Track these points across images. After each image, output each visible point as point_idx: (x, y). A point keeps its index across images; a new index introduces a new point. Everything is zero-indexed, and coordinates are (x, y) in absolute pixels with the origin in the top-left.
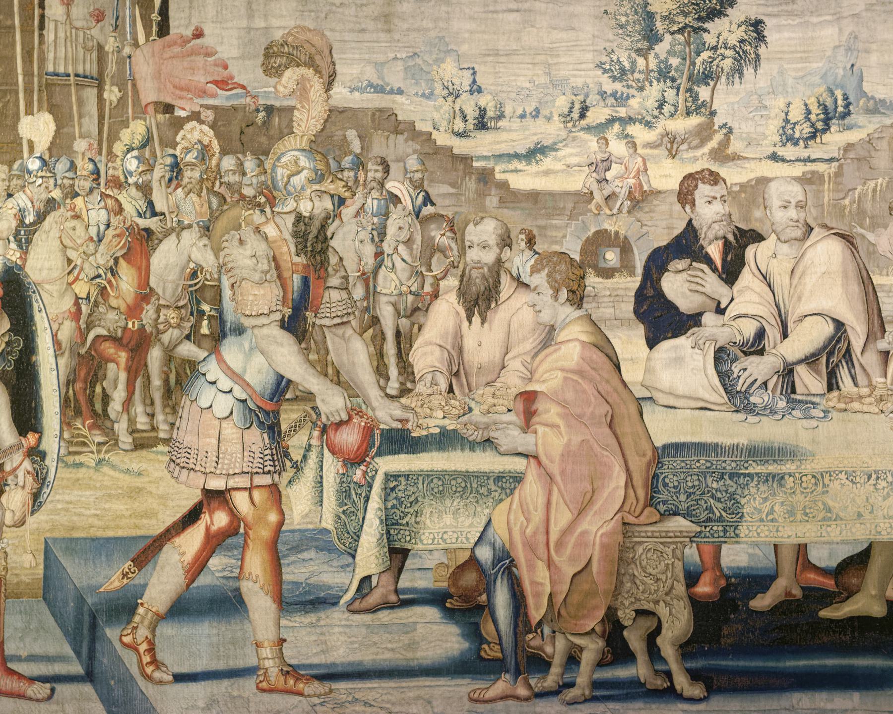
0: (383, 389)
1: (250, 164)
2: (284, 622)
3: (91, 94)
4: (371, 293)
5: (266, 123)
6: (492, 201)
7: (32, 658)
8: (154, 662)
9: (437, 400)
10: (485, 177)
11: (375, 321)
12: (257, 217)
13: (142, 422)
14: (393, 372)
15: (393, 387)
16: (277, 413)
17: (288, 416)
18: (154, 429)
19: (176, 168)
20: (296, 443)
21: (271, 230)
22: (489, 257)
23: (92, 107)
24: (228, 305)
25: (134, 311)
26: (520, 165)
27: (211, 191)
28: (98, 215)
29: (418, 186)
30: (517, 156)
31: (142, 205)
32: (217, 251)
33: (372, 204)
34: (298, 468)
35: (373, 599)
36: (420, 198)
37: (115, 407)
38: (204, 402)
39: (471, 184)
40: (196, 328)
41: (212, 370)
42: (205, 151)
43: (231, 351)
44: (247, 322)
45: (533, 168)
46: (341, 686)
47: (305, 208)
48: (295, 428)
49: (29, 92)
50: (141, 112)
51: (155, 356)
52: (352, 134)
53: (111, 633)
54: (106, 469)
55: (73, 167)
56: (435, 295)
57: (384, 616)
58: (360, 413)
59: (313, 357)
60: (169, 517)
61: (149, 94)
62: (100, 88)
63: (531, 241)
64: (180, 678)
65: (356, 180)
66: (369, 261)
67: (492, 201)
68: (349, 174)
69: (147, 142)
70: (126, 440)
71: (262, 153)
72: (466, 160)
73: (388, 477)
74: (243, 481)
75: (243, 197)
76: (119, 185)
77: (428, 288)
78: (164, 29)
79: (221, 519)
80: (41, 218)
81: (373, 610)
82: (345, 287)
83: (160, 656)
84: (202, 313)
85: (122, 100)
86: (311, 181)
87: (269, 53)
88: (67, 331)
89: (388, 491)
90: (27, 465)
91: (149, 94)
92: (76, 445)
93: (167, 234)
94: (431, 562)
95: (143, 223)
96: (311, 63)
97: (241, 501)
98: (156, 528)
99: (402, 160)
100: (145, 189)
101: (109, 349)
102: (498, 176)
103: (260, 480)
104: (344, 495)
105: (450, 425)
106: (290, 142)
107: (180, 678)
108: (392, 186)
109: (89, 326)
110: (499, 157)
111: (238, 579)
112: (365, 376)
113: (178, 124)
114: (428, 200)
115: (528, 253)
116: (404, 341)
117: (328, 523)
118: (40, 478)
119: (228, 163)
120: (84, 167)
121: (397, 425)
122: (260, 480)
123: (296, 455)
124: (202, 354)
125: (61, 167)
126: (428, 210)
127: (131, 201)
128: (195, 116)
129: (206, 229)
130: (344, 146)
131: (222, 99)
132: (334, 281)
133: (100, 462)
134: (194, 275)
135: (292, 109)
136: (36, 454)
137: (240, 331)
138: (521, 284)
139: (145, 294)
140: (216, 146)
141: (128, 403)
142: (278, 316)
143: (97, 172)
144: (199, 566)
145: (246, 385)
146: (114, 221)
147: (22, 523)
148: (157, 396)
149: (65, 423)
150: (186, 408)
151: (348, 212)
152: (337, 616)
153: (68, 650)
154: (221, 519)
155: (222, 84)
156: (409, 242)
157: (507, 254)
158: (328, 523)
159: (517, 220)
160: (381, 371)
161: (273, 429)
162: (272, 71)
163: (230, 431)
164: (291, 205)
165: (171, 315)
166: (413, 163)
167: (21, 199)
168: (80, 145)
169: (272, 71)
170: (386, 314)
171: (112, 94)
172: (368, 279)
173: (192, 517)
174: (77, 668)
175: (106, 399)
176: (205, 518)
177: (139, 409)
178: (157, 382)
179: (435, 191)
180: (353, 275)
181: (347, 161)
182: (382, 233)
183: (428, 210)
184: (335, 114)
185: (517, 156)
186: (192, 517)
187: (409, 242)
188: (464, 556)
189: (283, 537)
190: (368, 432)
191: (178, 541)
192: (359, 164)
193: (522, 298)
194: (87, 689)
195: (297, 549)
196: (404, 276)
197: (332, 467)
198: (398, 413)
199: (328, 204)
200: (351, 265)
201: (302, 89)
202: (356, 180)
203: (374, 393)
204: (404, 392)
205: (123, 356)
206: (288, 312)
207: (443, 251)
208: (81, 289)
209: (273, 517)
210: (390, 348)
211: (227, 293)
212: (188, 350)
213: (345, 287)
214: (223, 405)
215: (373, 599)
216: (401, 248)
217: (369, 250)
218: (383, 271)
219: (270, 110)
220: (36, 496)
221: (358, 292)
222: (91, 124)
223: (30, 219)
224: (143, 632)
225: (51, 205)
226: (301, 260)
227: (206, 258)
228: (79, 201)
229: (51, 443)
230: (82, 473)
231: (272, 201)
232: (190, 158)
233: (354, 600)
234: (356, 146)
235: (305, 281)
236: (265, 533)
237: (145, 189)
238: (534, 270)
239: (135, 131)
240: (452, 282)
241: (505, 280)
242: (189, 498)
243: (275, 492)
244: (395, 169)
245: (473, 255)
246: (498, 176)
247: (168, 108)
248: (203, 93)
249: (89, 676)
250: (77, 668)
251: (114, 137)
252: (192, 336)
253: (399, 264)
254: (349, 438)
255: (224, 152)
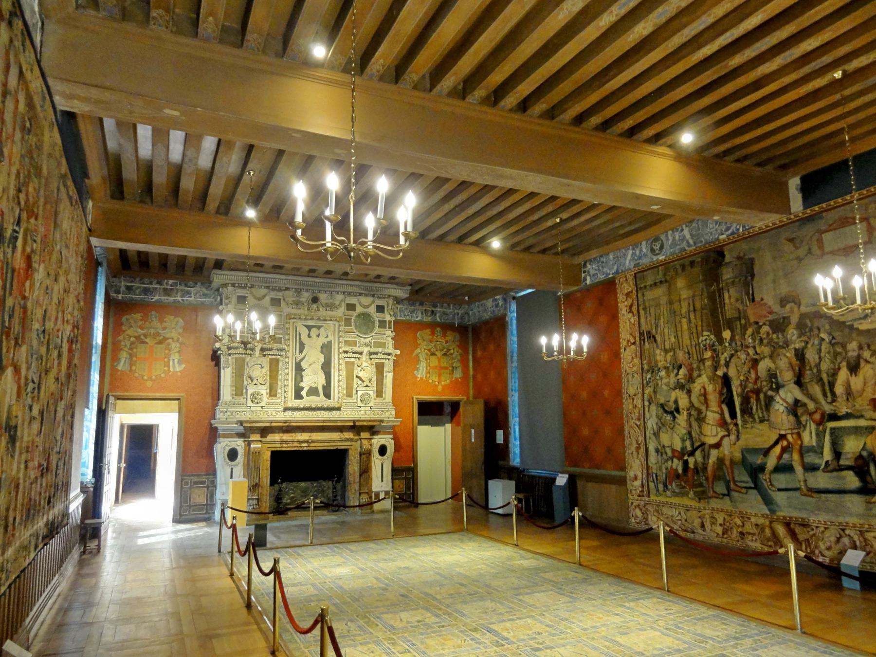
0: (826, 401)
1: (780, 336)
2: (806, 474)
3: (738, 323)
4: (819, 371)
5: (783, 322)
6: (854, 335)
7: (741, 482)
8: (771, 485)
9: (844, 403)
10: (851, 327)
11: (821, 379)
12: (784, 351)
13: (761, 415)
14: (829, 395)
15: (829, 399)
16: (796, 410)
17: (800, 411)
18: (764, 417)
19: (761, 340)
20: (803, 419)
21: (788, 355)
22: (855, 354)
23: (739, 326)
24: (779, 379)
25: (755, 383)
26: (862, 321)
27: (771, 345)
28: (743, 356)
29: (830, 334)
30: (860, 319)
31: (754, 352)
32: (774, 362)
33: (816, 342)
34: (805, 427)
35: (829, 468)
36: (831, 337)
37: (754, 411)
38: (776, 408)
39: (847, 331)
40: (771, 386)
41: (777, 399)
42: (768, 334)
43: (782, 392)
44: (785, 383)
45: (866, 321)
46: (823, 495)
47: (797, 346)
48: (802, 414)
49: (724, 324)
50: (750, 325)
51: (762, 396)
52: (808, 321)
53: (760, 476)
54: (754, 429)
55: (736, 344)
56: (839, 369)
57: (835, 474)
58: (820, 409)
59: (805, 392)
60: (771, 443)
61: (752, 320)
62: (740, 321)
63: (869, 346)
64: (780, 490)
65: (810, 335)
66: (817, 361)
67: (854, 335)
68: (808, 334)
69: (753, 334)
70: (757, 420)
71: (783, 331)
72: (844, 323)
73: (831, 429)
74: (789, 432)
75: (780, 346)
76: (747, 347)
77: (837, 367)
78: (753, 300)
79: (785, 443)
80: (730, 359)
81: (832, 471)
82: (811, 369)
83: (773, 483)
84: (773, 382)
85: (746, 323)
86: (798, 338)
87: (781, 301)
88: (739, 390)
89: (832, 434)
90: (735, 428)
91: (752, 320)
92: (745, 422)
93: (761, 359)
94: (849, 456)
95: (755, 357)
96: (793, 301)
97: (789, 437)
98: (767, 446)
99: (823, 326)
100: (754, 347)
101: (751, 394)
102: (855, 326)
103: (794, 431)
104: (817, 435)
105: (849, 411)
106: (791, 326)
107: (780, 490)
108: (822, 335)
109: (745, 388)
110: (856, 320)
111: (791, 461)
112: (820, 396)
113: (760, 327)
114: (833, 338)
115: (868, 351)
116: (832, 385)
117: (814, 444)
118: (738, 431)
119: (775, 336)
120: (739, 343)
121: (832, 412)
122: (794, 431)
123: (804, 423)
124: (774, 394)
125: (733, 344)
126: (833, 341)
127: (751, 351)
128: (764, 324)
129: (771, 357)
130: (806, 326)
131: (771, 317)
132: (808, 368)
133: (752, 427)
134: (769, 370)
135: (789, 317)
136: (736, 425)
137: (783, 386)
138: (867, 362)
139: (757, 378)
140: (771, 332)
141: (757, 409)
142: (793, 381)
143: (742, 345)
144: (780, 457)
145: (787, 402)
146: (748, 358)
147: (735, 444)
148: (764, 408)
149: (742, 416)
150: (772, 410)
151: (809, 346)
152: (819, 473)
153: (749, 479)
154: (785, 443)
155: (771, 313)
156: (829, 353)
157: (861, 352)
158: (814, 444)
159: (863, 340)
160: (825, 395)
161: (796, 415)
162: (783, 306)
163: (784, 417)
164: (792, 346)
165: (764, 383)
166: (827, 327)
167: (726, 355)
168: (737, 337)
169: (783, 306)
170: (824, 376)
171: (743, 322)
172: (818, 365)
173: (776, 443)
174: (753, 486)
175: (752, 409)
176: (780, 443)
177: (759, 411)
178: (763, 403)
179: (836, 334)
180: (813, 365)
181: (807, 330)
182: (820, 350)
183: (833, 341)
184: (803, 316)
185: (860, 319)
186: (776, 443)
187: (829, 353)
188: (858, 454)
189: (804, 449)
190: (823, 415)
191: (774, 449)
192: (811, 330)
193: (869, 366)
194: (755, 491)
195: (808, 452)
196: (829, 363)
197: (813, 427)
198: (833, 408)
199: (803, 344)
200: (811, 360)
201: (792, 311)
202: (810, 335)
203: (823, 402)
204: (834, 401)
205: (754, 396)
206: (796, 379)
207: (840, 353)
208: (742, 378)
209: (799, 442)
210: (827, 388)
211: (778, 375)
212: (770, 393)
213: (811, 369)
214: (782, 409)
215: (829, 468)
216: (827, 355)
217: (817, 357)
218: (822, 363)
219: (784, 318)
220: (738, 436)
221: (815, 371)
222: (739, 331)
223: (728, 360)
224: (768, 476)
225: (732, 356)
226: (798, 362)
227: (772, 366)
228: (739, 353)
229: (739, 422)
230: (748, 430)
231: (788, 346)
232: (764, 336)
233: (824, 468)
234: (809, 324)
235: (799, 369)
236: (797, 447)
237: (754, 347)
238: (871, 356)
239: (750, 331)
240: (844, 364)
241: (862, 361)
242: (775, 437)
243: (799, 435)
244: (822, 330)
245: (850, 354)
246: (855, 326)
247: (757, 323)
248: (765, 316)
249: (756, 488)
250: (753, 486)
251: (745, 334)
252: (771, 389)
253: (827, 360)
254: (817, 416)
255: (773, 333)
